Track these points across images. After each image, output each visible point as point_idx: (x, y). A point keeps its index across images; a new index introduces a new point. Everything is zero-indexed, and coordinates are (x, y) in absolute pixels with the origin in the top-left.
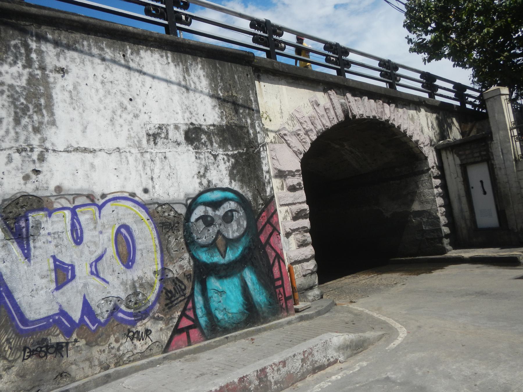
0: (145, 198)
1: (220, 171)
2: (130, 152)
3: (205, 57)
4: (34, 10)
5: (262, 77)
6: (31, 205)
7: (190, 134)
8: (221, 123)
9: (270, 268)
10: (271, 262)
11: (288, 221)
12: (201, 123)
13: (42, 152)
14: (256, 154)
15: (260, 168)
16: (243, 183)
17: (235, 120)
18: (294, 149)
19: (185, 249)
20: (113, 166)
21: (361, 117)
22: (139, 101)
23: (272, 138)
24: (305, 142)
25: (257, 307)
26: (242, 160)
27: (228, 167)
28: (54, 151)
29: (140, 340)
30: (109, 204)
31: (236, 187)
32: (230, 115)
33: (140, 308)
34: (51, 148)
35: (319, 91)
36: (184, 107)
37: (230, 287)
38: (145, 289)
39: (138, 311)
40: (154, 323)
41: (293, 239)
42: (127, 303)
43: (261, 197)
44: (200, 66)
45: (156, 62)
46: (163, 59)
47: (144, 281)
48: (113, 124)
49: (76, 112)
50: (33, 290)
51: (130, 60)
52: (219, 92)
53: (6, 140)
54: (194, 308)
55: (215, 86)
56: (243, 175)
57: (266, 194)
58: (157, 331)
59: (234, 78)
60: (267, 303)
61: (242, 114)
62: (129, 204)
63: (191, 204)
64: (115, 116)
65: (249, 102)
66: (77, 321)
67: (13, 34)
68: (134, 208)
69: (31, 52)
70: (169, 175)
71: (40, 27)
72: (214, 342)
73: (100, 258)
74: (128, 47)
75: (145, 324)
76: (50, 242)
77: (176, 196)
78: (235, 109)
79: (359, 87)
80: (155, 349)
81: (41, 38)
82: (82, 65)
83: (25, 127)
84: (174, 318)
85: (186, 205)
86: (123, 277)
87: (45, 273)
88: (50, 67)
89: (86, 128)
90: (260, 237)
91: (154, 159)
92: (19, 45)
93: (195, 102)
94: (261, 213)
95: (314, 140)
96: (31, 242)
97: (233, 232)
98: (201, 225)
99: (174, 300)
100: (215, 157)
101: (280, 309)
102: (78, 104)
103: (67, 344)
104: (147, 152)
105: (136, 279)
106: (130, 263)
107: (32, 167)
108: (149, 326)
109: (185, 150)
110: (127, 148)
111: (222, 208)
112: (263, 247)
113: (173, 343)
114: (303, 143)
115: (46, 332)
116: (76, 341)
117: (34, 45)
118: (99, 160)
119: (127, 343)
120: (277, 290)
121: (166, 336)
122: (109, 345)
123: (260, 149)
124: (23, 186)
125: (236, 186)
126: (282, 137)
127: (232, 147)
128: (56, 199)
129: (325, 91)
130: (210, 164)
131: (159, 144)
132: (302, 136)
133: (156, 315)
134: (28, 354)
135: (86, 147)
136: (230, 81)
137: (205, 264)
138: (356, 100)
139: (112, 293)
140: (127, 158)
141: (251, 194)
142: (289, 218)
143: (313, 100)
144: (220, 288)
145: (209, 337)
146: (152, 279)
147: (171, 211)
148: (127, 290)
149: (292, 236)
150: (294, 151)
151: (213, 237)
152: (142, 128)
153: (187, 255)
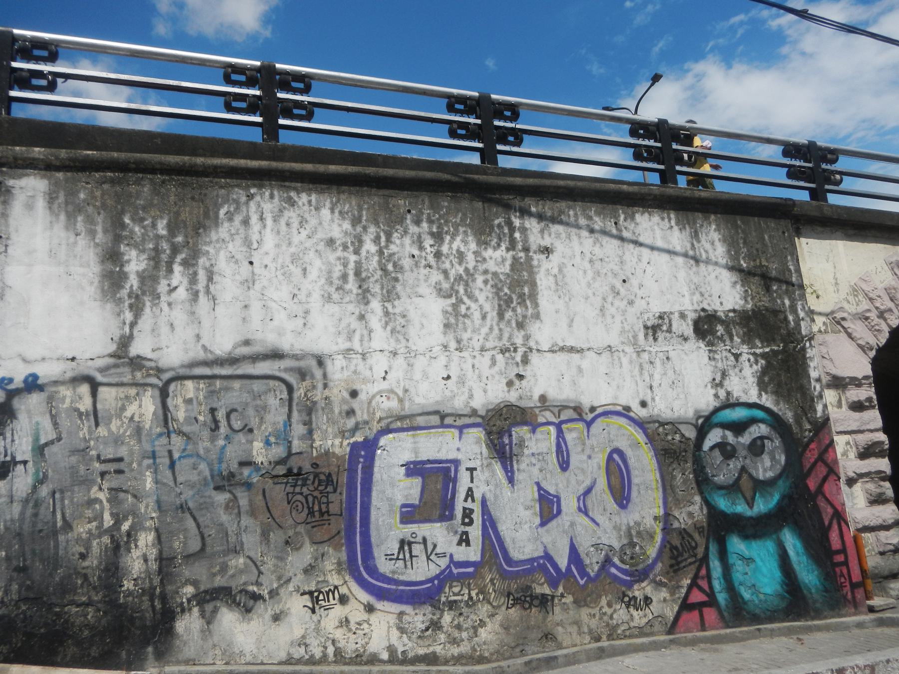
0: (643, 413)
1: (744, 378)
2: (623, 351)
3: (720, 214)
4: (518, 181)
6: (515, 417)
7: (701, 324)
8: (744, 306)
9: (825, 532)
10: (827, 523)
11: (851, 460)
12: (716, 308)
14: (799, 352)
17: (765, 302)
18: (860, 342)
19: (696, 488)
20: (603, 369)
22: (634, 282)
23: (821, 325)
24: (878, 330)
25: (805, 592)
26: (778, 362)
28: (538, 350)
29: (637, 610)
30: (599, 420)
32: (758, 294)
33: (637, 565)
34: (535, 347)
36: (693, 287)
37: (761, 554)
38: (643, 539)
39: (634, 568)
40: (656, 589)
41: (860, 489)
42: (621, 556)
43: (807, 418)
44: (714, 227)
45: (656, 227)
46: (664, 223)
47: (642, 529)
48: (603, 315)
49: (561, 301)
50: (516, 523)
51: (623, 229)
52: (742, 262)
53: (490, 339)
54: (709, 577)
55: (736, 253)
56: (779, 385)
58: (659, 601)
59: (764, 239)
60: (821, 587)
61: (776, 291)
62: (623, 421)
64: (605, 304)
65: (787, 273)
66: (564, 570)
67: (496, 213)
68: (629, 427)
69: (514, 232)
70: (673, 383)
71: (523, 200)
72: (740, 632)
73: (588, 491)
74: (621, 211)
75: (644, 588)
76: (534, 465)
77: (682, 412)
80: (657, 627)
81: (524, 212)
82: (567, 240)
83: (509, 322)
84: (682, 587)
85: (696, 426)
86: (616, 519)
87: (529, 503)
88: (534, 247)
89: (572, 321)
90: (808, 481)
91: (653, 360)
92: (503, 224)
93: (708, 278)
94: (808, 444)
95: (894, 326)
96: (515, 463)
97: (765, 470)
99: (682, 561)
100: (737, 357)
101: (843, 600)
102: (564, 291)
103: (553, 597)
104: (645, 351)
105: (632, 524)
106: (625, 502)
107: (516, 371)
108: (649, 592)
109: (695, 347)
110: (620, 345)
111: (747, 433)
112: (813, 497)
113: (681, 622)
114: (876, 331)
115: (530, 577)
116: (562, 596)
117: (517, 222)
118: (588, 361)
119: (621, 611)
120: (837, 570)
121: (672, 610)
122: (600, 609)
124: (507, 394)
125: (767, 401)
126: (838, 323)
127: (762, 342)
128: (540, 411)
131: (660, 339)
132: (873, 320)
133: (658, 578)
134: (512, 602)
135: (573, 345)
137: (723, 514)
139: (603, 539)
140: (619, 359)
142: (852, 454)
144: (747, 554)
145: (730, 624)
146: (652, 527)
147: (676, 433)
148: (620, 537)
151: (734, 475)
152: (638, 318)
153: (697, 499)
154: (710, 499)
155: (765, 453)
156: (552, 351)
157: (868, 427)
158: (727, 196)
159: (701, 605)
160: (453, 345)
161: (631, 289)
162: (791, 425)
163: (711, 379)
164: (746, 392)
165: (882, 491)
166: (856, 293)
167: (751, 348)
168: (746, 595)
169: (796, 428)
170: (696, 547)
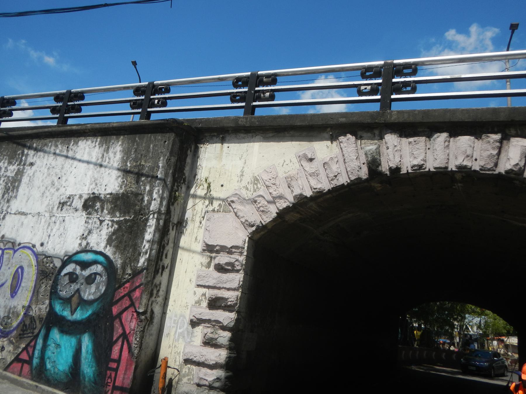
0: (39, 249)
2: (44, 215)
3: (127, 135)
4: (30, 132)
5: (228, 138)
8: (118, 191)
9: (112, 344)
10: (114, 339)
12: (101, 192)
13: (5, 214)
15: (142, 236)
16: (117, 249)
18: (242, 220)
19: (49, 296)
20: (32, 225)
21: (414, 170)
22: (64, 179)
24: (263, 211)
25: (81, 378)
26: (125, 227)
27: (109, 233)
28: (10, 213)
30: (20, 250)
31: (109, 252)
32: (131, 183)
34: (9, 212)
35: (322, 139)
36: (93, 180)
43: (131, 266)
48: (43, 196)
51: (70, 150)
54: (34, 347)
55: (126, 159)
56: (120, 242)
57: (138, 264)
58: (7, 351)
59: (149, 147)
60: (92, 379)
61: (142, 182)
62: (29, 252)
63: (66, 260)
65: (156, 168)
68: (31, 256)
70: (61, 235)
71: (32, 140)
72: (27, 383)
75: (4, 341)
77: (58, 252)
78: (137, 177)
79: (419, 119)
82: (43, 159)
83: (5, 199)
84: (20, 348)
85: (62, 260)
88: (28, 163)
89: (28, 199)
90: (113, 308)
91: (56, 221)
93: (104, 175)
95: (281, 208)
97: (89, 294)
99: (25, 334)
100: (101, 222)
104: (54, 216)
105: (12, 307)
106: (14, 294)
109: (80, 215)
111: (89, 269)
112: (112, 319)
113: (11, 366)
117: (26, 151)
120: (108, 372)
121: (11, 358)
123: (150, 216)
125: (109, 252)
126: (230, 205)
127: (120, 214)
129: (333, 138)
130: (94, 228)
136: (143, 151)
137: (56, 314)
138: (410, 143)
142: (205, 304)
143: (301, 154)
148: (5, 312)
149: (200, 327)
150: (241, 222)
152: (58, 198)
153: (47, 302)
154: (53, 304)
155: (94, 283)
156: (15, 214)
157: (225, 286)
158: (128, 123)
159: (23, 362)
161: (61, 182)
162: (117, 269)
164: (98, 244)
165: (214, 337)
166: (256, 182)
167: (111, 217)
168: (49, 366)
169: (120, 271)
170: (35, 329)
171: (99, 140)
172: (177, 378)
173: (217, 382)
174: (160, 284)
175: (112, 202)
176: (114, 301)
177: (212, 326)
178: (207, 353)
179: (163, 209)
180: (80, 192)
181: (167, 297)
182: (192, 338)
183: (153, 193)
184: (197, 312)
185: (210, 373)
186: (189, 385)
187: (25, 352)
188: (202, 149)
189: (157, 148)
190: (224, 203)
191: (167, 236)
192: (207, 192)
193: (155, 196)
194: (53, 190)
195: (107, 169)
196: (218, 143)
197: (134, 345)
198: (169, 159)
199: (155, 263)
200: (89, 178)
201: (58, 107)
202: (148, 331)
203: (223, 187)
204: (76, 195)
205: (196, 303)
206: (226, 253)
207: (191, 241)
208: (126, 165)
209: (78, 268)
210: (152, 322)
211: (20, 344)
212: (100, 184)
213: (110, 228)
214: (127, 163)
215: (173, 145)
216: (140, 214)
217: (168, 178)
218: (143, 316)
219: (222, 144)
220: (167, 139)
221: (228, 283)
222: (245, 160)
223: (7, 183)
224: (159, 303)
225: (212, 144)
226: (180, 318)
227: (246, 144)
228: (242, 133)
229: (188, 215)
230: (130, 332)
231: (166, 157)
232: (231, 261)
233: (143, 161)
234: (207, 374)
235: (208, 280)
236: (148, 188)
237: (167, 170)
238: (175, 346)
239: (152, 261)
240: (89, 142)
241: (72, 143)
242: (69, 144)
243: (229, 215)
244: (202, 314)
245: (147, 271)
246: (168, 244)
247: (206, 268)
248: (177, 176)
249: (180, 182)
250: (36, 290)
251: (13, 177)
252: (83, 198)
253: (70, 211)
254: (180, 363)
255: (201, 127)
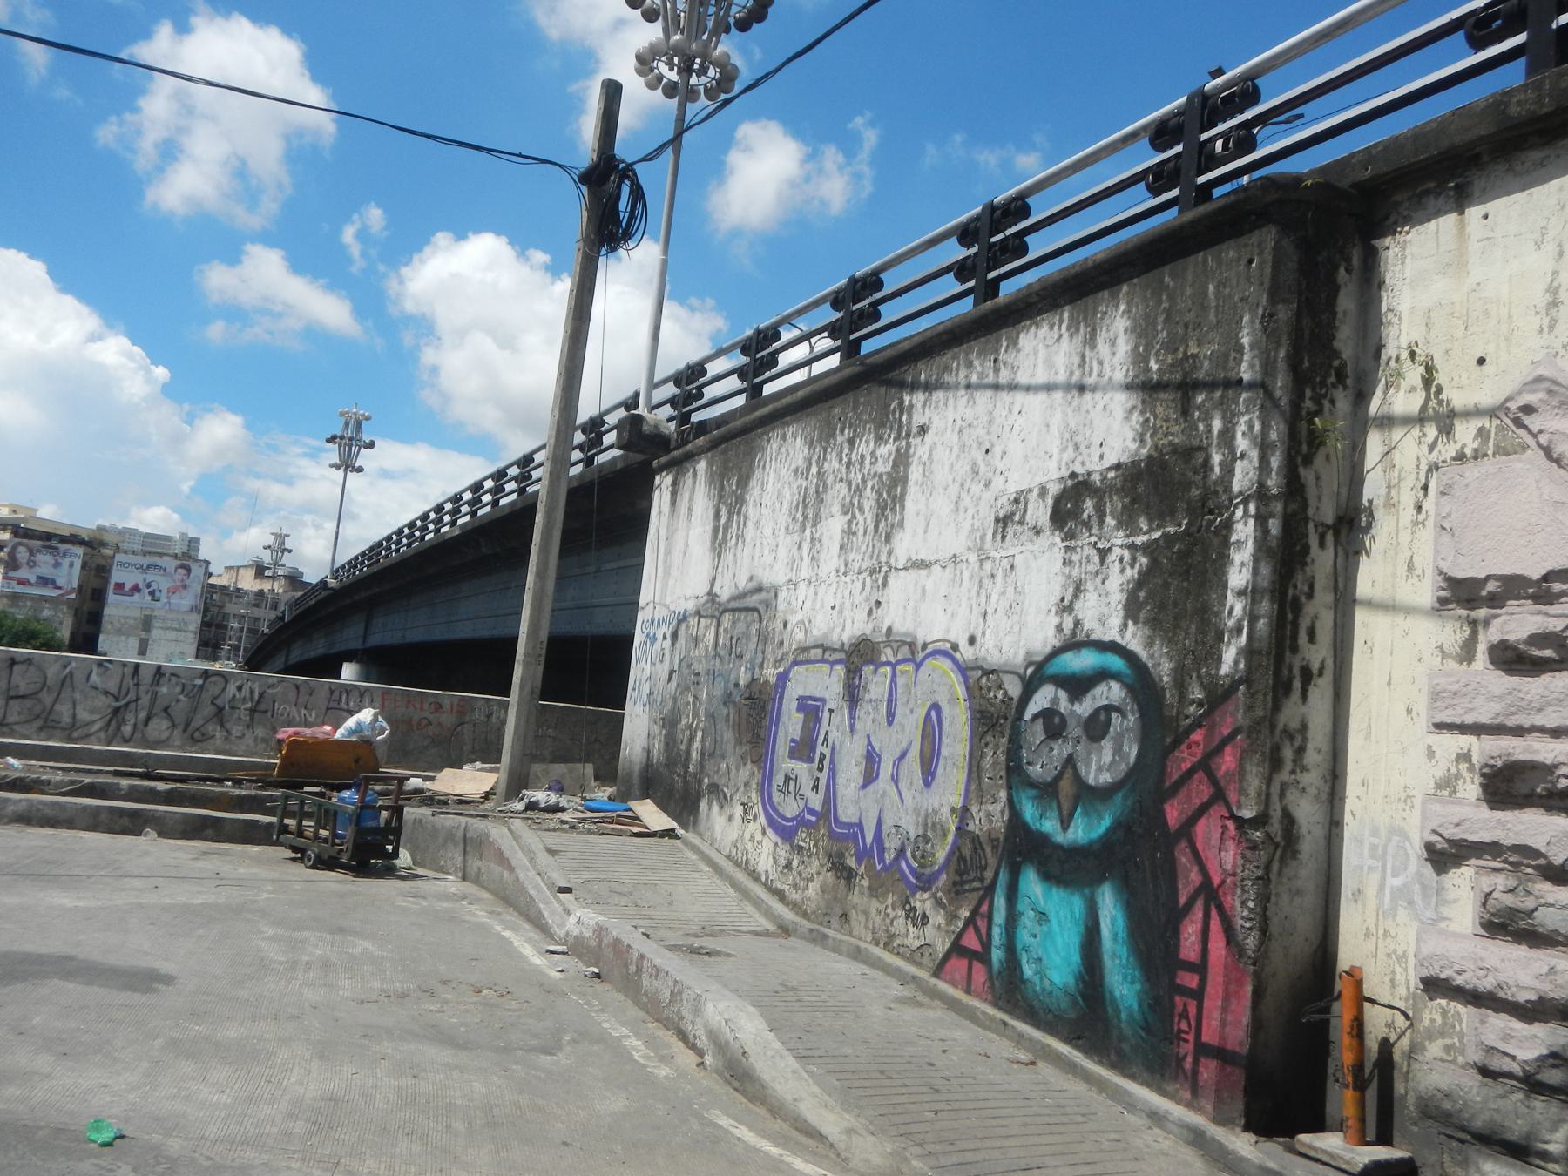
0: (967, 653)
3: (1138, 276)
5: (1478, 184)
7: (1064, 501)
10: (1182, 900)
11: (1461, 802)
14: (1216, 533)
19: (1004, 780)
22: (997, 450)
25: (1110, 1010)
26: (1170, 559)
27: (1128, 582)
30: (927, 662)
32: (1166, 420)
36: (1067, 436)
37: (1062, 913)
43: (1199, 677)
48: (957, 510)
56: (1162, 607)
57: (1218, 669)
58: (934, 926)
59: (1205, 294)
60: (1138, 1017)
62: (944, 664)
65: (1233, 354)
72: (984, 1013)
73: (903, 756)
75: (924, 901)
78: (1182, 398)
80: (926, 960)
85: (1022, 678)
88: (914, 430)
90: (1167, 807)
97: (1100, 769)
98: (1037, 733)
100: (1104, 553)
105: (930, 810)
111: (1089, 696)
117: (907, 398)
120: (1178, 999)
121: (943, 944)
123: (1234, 512)
125: (1134, 639)
126: (1519, 423)
127: (1150, 521)
130: (1088, 577)
133: (939, 894)
137: (1025, 827)
141: (1172, 665)
142: (1471, 789)
149: (1463, 869)
153: (1003, 794)
154: (1015, 799)
155: (1108, 737)
156: (906, 569)
157: (1538, 720)
159: (971, 955)
160: (842, 569)
162: (1163, 689)
163: (1059, 598)
164: (1102, 621)
165: (1519, 905)
167: (1127, 536)
168: (1028, 971)
169: (1172, 696)
170: (984, 868)
171: (1066, 315)
172: (1405, 1042)
173: (1554, 1066)
174: (1304, 727)
175: (1123, 489)
176: (1167, 784)
177: (1510, 868)
178: (1503, 960)
179: (1274, 482)
180: (1039, 479)
181: (1338, 773)
182: (1441, 909)
183: (1233, 437)
184: (1443, 816)
185: (1525, 1033)
186: (1453, 1067)
187: (971, 932)
188: (1391, 253)
189: (1227, 291)
190: (1496, 422)
191: (1303, 570)
192: (1428, 399)
193: (1242, 444)
194: (976, 489)
195: (1098, 395)
196: (1446, 213)
197: (1241, 922)
198: (1271, 315)
199: (1272, 661)
200: (1056, 434)
201: (970, 261)
202: (1285, 880)
203: (1483, 367)
204: (1030, 490)
205: (1439, 786)
206: (1530, 602)
207: (1394, 575)
208: (1148, 369)
209: (1062, 694)
210: (1295, 854)
211: (957, 909)
212: (1086, 443)
213: (1128, 567)
214: (1147, 361)
215: (1276, 266)
216: (1206, 510)
217: (1276, 378)
218: (1256, 830)
219: (1462, 213)
220: (1256, 251)
221: (1550, 709)
222: (1560, 245)
223: (879, 494)
224: (1312, 791)
225: (1421, 223)
226: (1389, 840)
227: (1555, 184)
228: (1532, 147)
229: (1373, 488)
230: (1223, 882)
231: (1260, 311)
232: (1551, 628)
233: (1191, 344)
234: (1512, 1037)
235: (1469, 706)
236: (1217, 424)
237: (1267, 351)
238: (1386, 933)
239: (1260, 653)
240: (1044, 330)
241: (1004, 344)
242: (997, 351)
243: (1519, 460)
244: (1467, 824)
245: (1248, 688)
246: (1310, 595)
247: (1461, 663)
248: (1306, 364)
249: (1323, 384)
250: (975, 764)
251: (889, 474)
252: (1050, 496)
253: (1023, 538)
254: (1408, 988)
255: (1372, 179)
